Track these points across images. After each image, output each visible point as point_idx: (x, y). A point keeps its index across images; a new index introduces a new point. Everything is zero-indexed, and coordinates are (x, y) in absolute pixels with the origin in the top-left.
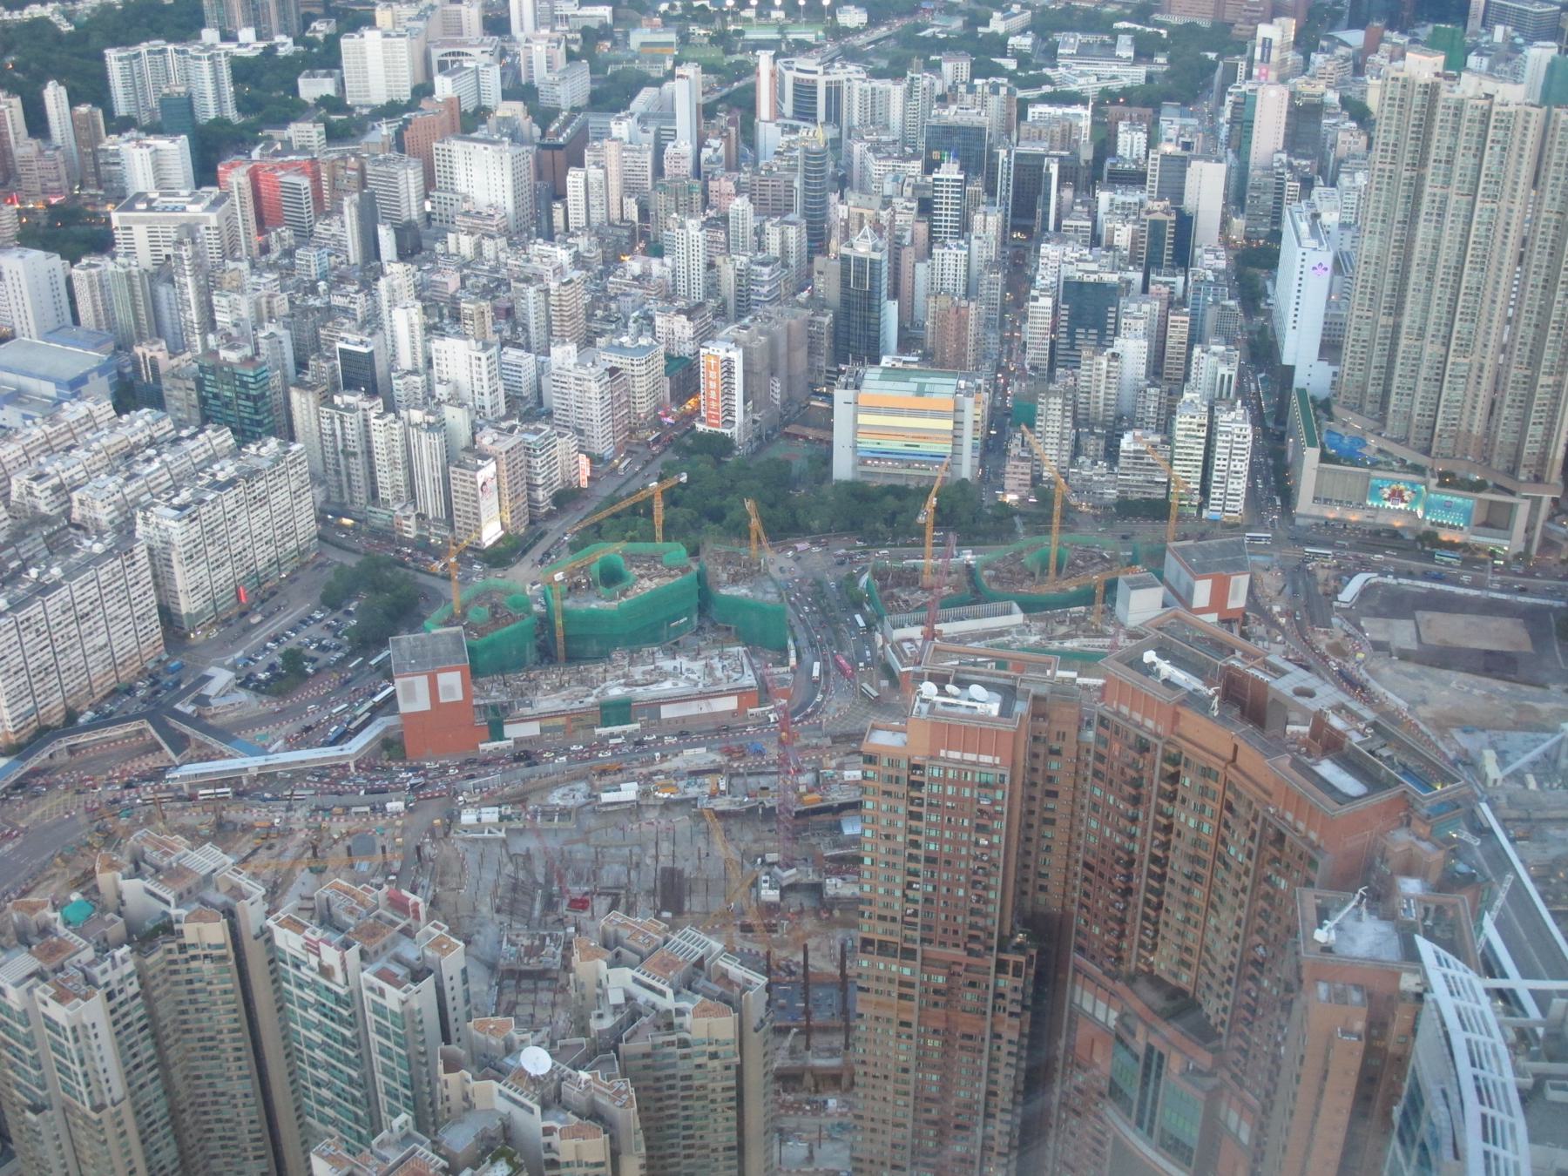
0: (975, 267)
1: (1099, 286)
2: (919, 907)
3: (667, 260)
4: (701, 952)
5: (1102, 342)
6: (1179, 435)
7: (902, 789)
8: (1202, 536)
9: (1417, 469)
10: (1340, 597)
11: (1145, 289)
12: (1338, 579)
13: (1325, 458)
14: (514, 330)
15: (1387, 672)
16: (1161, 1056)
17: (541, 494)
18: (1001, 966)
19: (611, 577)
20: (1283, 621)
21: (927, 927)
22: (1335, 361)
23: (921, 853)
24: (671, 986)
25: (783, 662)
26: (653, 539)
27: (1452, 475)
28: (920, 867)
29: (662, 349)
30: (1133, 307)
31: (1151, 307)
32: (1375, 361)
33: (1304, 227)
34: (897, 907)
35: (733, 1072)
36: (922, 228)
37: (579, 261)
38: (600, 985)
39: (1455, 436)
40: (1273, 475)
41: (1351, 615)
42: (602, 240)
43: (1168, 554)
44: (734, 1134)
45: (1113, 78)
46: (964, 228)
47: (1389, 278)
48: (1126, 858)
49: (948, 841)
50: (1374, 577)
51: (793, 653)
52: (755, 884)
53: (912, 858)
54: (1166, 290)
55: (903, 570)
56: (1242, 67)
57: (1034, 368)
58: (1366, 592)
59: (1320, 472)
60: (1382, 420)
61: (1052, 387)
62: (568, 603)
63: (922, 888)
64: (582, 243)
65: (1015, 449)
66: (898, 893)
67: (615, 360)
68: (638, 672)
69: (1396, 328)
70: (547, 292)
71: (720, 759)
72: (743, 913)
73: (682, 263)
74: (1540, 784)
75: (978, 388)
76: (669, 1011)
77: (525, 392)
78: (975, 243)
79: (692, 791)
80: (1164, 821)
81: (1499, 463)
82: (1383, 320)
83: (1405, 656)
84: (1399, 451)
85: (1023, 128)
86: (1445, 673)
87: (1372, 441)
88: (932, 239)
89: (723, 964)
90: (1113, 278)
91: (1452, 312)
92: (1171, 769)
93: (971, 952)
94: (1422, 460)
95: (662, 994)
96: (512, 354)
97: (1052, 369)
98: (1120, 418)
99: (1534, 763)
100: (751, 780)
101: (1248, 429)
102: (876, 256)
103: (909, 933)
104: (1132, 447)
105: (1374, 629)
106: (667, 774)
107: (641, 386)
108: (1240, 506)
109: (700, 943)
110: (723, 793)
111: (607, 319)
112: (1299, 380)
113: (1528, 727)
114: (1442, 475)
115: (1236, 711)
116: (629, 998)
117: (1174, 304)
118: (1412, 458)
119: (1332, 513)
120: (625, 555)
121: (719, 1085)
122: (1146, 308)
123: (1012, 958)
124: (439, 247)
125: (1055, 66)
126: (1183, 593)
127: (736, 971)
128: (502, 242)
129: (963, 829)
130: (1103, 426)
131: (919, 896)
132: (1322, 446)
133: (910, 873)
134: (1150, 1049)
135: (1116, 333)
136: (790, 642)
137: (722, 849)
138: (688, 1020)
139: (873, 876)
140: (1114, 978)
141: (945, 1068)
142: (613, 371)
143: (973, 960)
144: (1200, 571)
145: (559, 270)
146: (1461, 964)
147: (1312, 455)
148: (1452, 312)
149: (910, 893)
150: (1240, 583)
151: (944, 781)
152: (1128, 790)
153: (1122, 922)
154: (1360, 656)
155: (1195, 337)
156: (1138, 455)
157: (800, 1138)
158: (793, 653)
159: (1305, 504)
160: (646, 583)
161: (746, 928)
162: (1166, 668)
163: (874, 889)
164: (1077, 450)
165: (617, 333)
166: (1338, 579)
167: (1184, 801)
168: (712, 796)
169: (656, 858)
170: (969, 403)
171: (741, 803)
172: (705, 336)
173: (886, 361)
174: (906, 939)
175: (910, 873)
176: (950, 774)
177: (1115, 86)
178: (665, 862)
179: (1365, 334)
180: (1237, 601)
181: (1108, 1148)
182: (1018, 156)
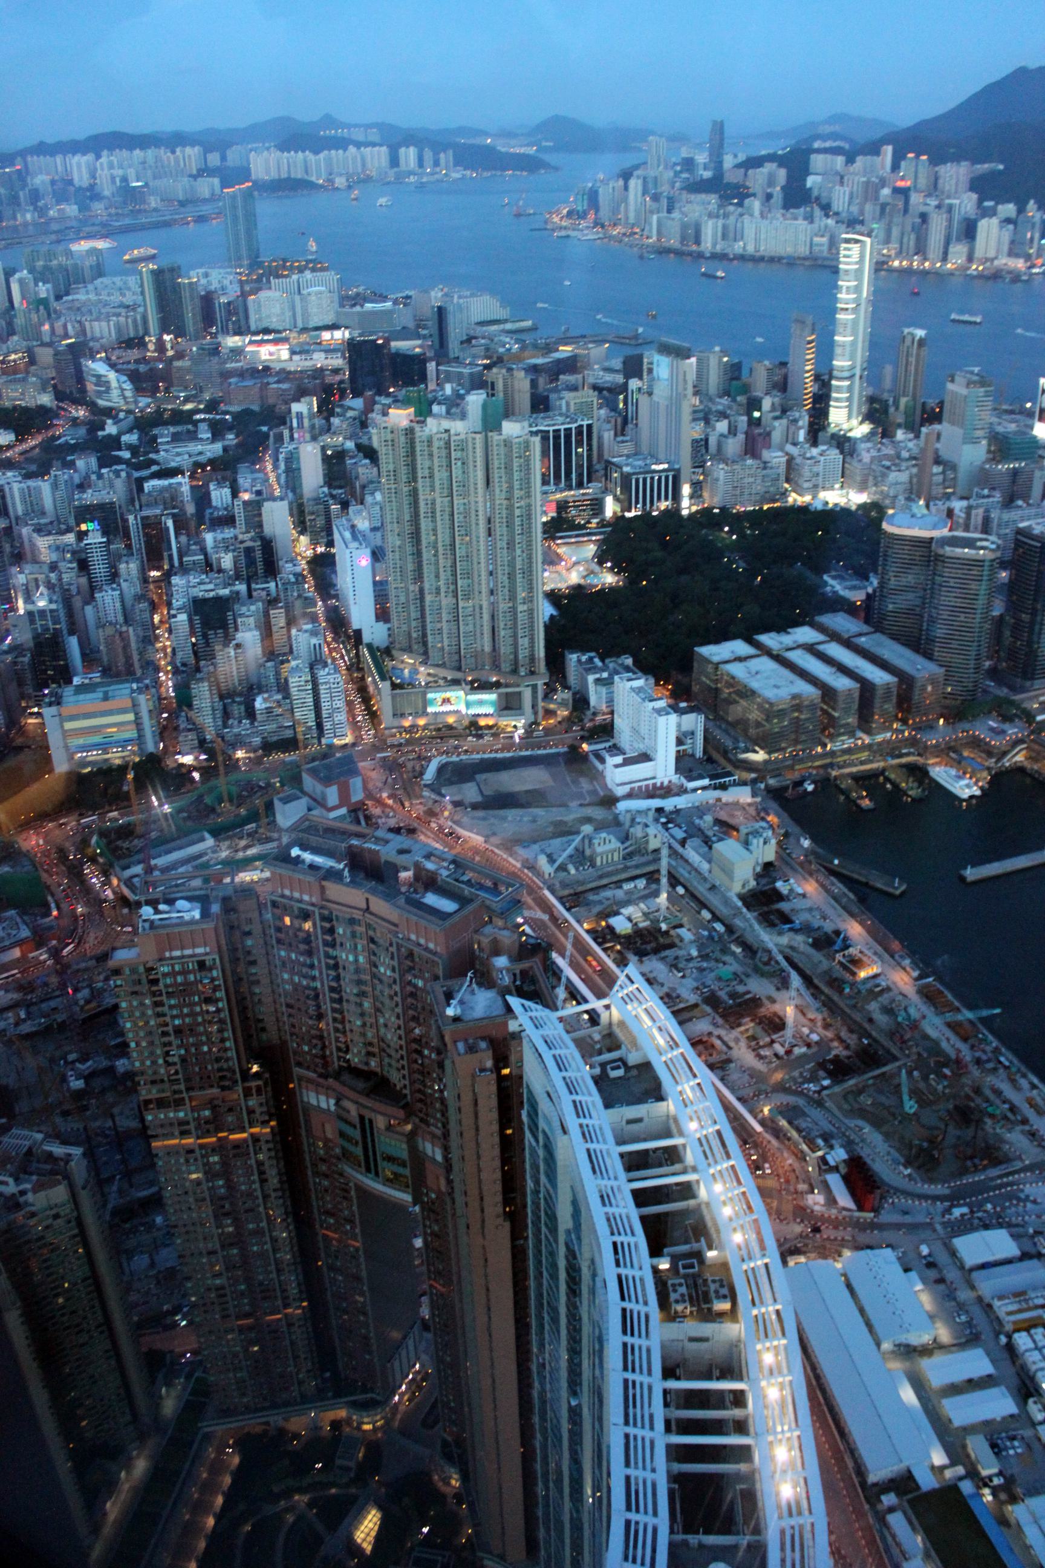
1: (218, 599)
2: (178, 1067)
4: (27, 1143)
5: (227, 639)
6: (294, 691)
7: (145, 988)
10: (425, 777)
11: (250, 596)
15: (465, 820)
16: (371, 1121)
18: (247, 1093)
20: (390, 802)
21: (187, 1080)
23: (170, 1029)
24: (11, 1175)
25: (48, 913)
28: (172, 1038)
30: (244, 609)
32: (413, 615)
33: (347, 535)
34: (162, 1071)
35: (73, 1223)
36: (83, 580)
43: (305, 776)
44: (86, 1268)
45: (200, 453)
46: (114, 576)
47: (410, 559)
48: (312, 993)
49: (187, 1015)
50: (444, 759)
51: (53, 905)
52: (64, 1079)
53: (165, 1034)
54: (264, 593)
56: (286, 433)
57: (184, 665)
58: (441, 769)
59: (394, 697)
61: (198, 676)
63: (176, 1053)
66: (161, 1061)
69: (422, 591)
71: (16, 996)
72: (61, 1103)
74: (577, 869)
75: (147, 687)
76: (13, 1195)
78: (124, 585)
80: (332, 962)
81: (506, 667)
82: (411, 588)
83: (475, 807)
85: (144, 499)
86: (502, 812)
88: (92, 588)
89: (47, 1148)
90: (225, 592)
92: (327, 925)
93: (223, 1088)
94: (458, 675)
95: (6, 1183)
98: (251, 688)
99: (571, 856)
100: (43, 1005)
102: (53, 606)
103: (176, 1087)
104: (264, 706)
109: (25, 1138)
110: (24, 1020)
112: (366, 638)
114: (472, 682)
115: (362, 875)
117: (272, 602)
122: (253, 608)
123: (253, 1084)
125: (157, 452)
126: (319, 799)
127: (58, 1150)
129: (196, 1004)
130: (240, 695)
131: (176, 1059)
133: (165, 1045)
134: (362, 1118)
135: (236, 629)
136: (49, 898)
137: (31, 1062)
138: (30, 1197)
139: (141, 1053)
144: (327, 781)
146: (539, 1007)
148: (454, 574)
149: (170, 1059)
151: (173, 974)
152: (303, 947)
154: (446, 813)
156: (269, 710)
157: (142, 1252)
158: (53, 905)
161: (65, 1114)
162: (308, 857)
163: (143, 1063)
164: (226, 715)
167: (342, 944)
168: (17, 1024)
170: (142, 699)
171: (40, 1024)
173: (76, 681)
174: (175, 1092)
176: (177, 968)
177: (202, 459)
181: (353, 1193)
182: (143, 518)
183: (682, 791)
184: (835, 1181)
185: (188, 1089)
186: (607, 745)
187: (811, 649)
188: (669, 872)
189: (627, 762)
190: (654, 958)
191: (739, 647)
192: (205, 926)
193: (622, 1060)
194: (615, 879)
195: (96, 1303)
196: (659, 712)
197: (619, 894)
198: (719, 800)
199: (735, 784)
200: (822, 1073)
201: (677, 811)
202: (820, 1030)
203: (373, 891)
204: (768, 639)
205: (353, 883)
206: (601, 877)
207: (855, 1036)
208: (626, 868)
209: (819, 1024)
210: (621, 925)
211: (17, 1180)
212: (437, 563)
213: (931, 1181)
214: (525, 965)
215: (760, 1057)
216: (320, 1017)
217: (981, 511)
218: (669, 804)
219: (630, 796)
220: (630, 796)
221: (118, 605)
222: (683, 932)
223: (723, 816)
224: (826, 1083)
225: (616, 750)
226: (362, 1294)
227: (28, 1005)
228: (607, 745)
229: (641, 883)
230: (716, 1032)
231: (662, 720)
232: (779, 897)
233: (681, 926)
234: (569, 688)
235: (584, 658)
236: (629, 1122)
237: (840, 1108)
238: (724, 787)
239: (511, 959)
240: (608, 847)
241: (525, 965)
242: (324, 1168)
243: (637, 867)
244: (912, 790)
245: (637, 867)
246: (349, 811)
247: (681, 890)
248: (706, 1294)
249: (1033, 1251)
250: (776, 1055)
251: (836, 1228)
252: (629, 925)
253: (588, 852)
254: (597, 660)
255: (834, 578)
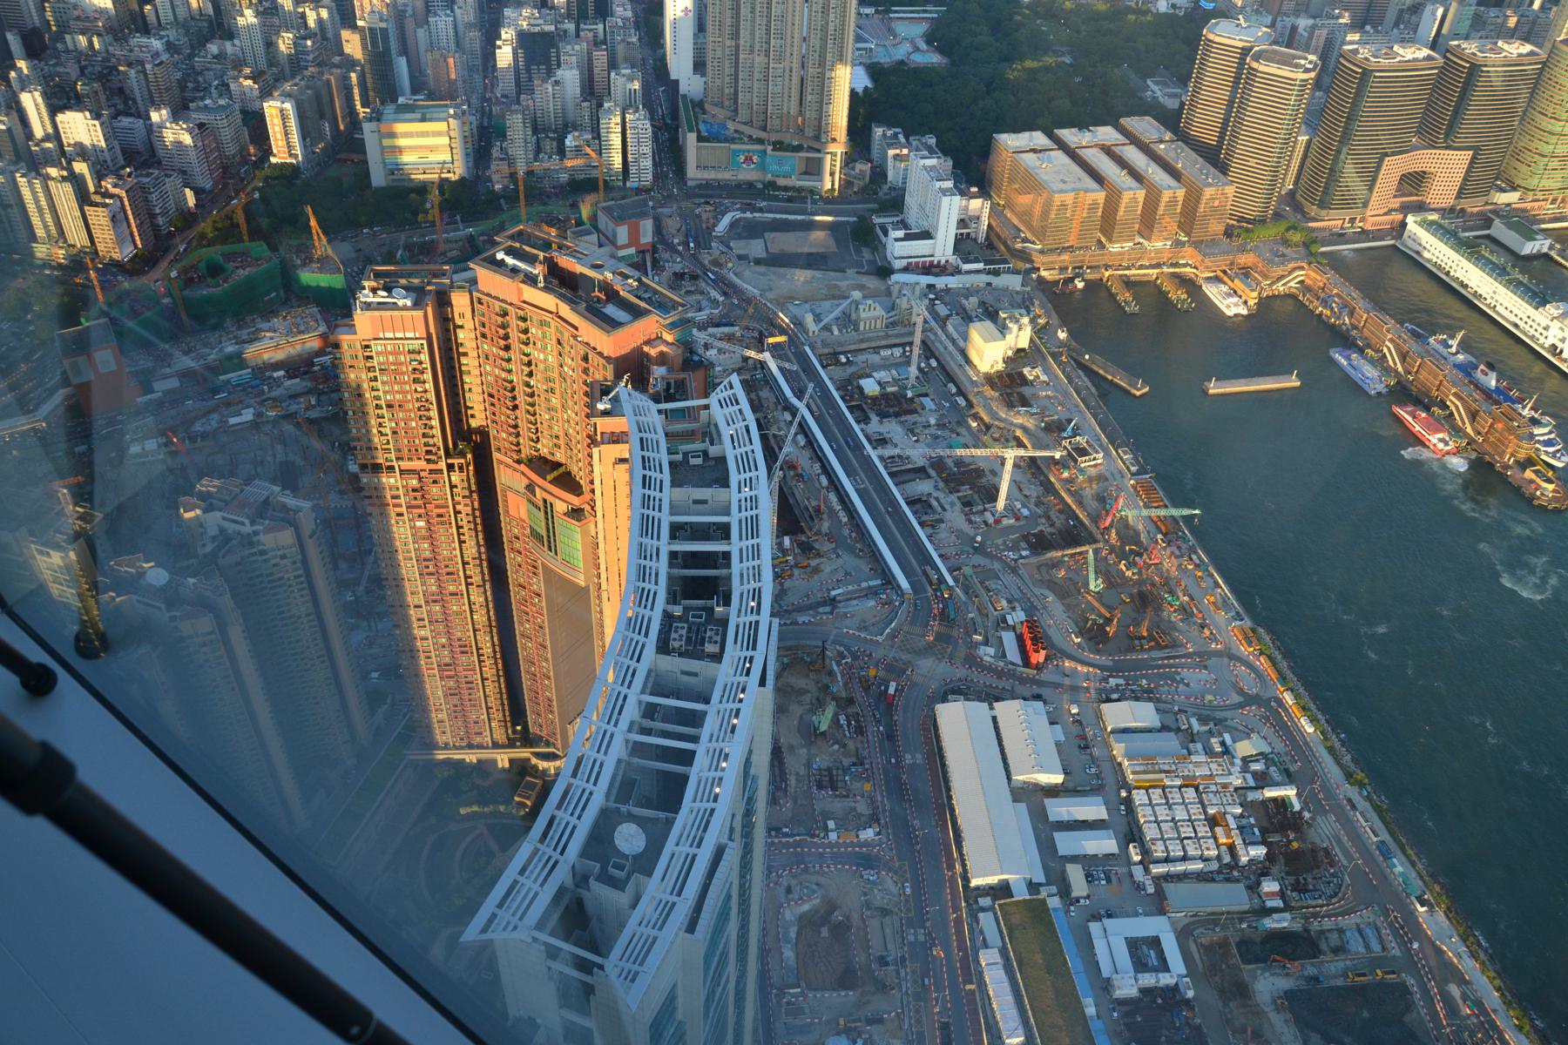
0: (461, 28)
1: (544, 35)
3: (236, 42)
5: (550, 73)
8: (624, 198)
9: (760, 141)
11: (578, 36)
12: (715, 217)
13: (700, 139)
14: (125, 102)
15: (747, 273)
17: (160, 220)
18: (450, 467)
19: (215, 270)
22: (703, 75)
23: (383, 403)
26: (241, 240)
27: (781, 143)
28: (384, 411)
29: (237, 107)
31: (581, 47)
32: (727, 71)
37: (170, 47)
38: (201, 525)
39: (780, 117)
40: (669, 152)
41: (724, 241)
42: (187, 32)
47: (729, 14)
50: (738, 215)
55: (425, 243)
58: (733, 225)
59: (698, 148)
60: (736, 111)
62: (187, 292)
63: (389, 426)
64: (172, 34)
65: (496, 152)
67: (202, 117)
68: (244, 334)
69: (737, 46)
70: (144, 72)
73: (247, 43)
75: (464, 112)
77: (140, 148)
78: (458, 11)
79: (294, 408)
80: (526, 359)
81: (809, 132)
82: (728, 43)
83: (758, 262)
84: (747, 130)
87: (731, 126)
90: (552, 28)
91: (768, 33)
93: (428, 461)
95: (243, 524)
96: (126, 121)
97: (519, 93)
98: (566, 126)
101: (648, 125)
102: (383, 25)
105: (739, 247)
106: (274, 400)
107: (226, 135)
108: (650, 177)
111: (196, 89)
112: (683, 89)
113: (834, 297)
114: (774, 144)
115: (556, 282)
116: (222, 530)
117: (596, 43)
118: (757, 134)
119: (711, 175)
120: (223, 255)
121: (291, 575)
122: (577, 47)
123: (455, 462)
124: (60, 46)
126: (610, 235)
127: (290, 501)
128: (109, 38)
132: (699, 132)
133: (379, 417)
134: (545, 501)
135: (559, 66)
138: (262, 537)
140: (519, 462)
141: (431, 537)
142: (201, 126)
143: (433, 467)
144: (619, 220)
145: (156, 54)
147: (692, 138)
148: (768, 33)
150: (647, 226)
151: (387, 353)
152: (502, 343)
153: (516, 427)
155: (613, 65)
159: (692, 172)
160: (241, 272)
162: (510, 261)
163: (359, 430)
165: (202, 99)
166: (715, 217)
168: (307, 409)
169: (274, 456)
172: (266, 93)
173: (401, 100)
175: (379, 417)
178: (280, 457)
179: (719, 53)
180: (647, 237)
183: (957, 271)
184: (1009, 639)
185: (398, 459)
186: (895, 219)
187: (1108, 151)
188: (923, 342)
189: (908, 237)
190: (893, 420)
191: (1039, 139)
192: (414, 313)
193: (705, 453)
194: (874, 344)
195: (318, 636)
196: (944, 192)
197: (875, 359)
198: (989, 284)
199: (1009, 271)
200: (1023, 545)
201: (947, 290)
202: (1032, 506)
203: (562, 297)
204: (1069, 135)
205: (546, 289)
206: (862, 341)
207: (1062, 517)
208: (887, 336)
209: (1033, 500)
210: (870, 386)
211: (253, 523)
212: (753, 21)
213: (1098, 652)
214: (682, 375)
215: (970, 521)
216: (515, 407)
217: (1324, 32)
218: (941, 282)
219: (906, 270)
220: (906, 270)
221: (451, 31)
222: (927, 401)
223: (989, 299)
224: (1024, 553)
225: (904, 225)
226: (546, 660)
227: (320, 394)
228: (895, 219)
229: (898, 352)
230: (935, 495)
231: (946, 200)
232: (1024, 381)
233: (926, 395)
234: (870, 161)
235: (889, 133)
236: (696, 502)
237: (1031, 577)
238: (996, 273)
239: (670, 370)
240: (872, 314)
241: (682, 375)
242: (517, 545)
243: (896, 336)
244: (1178, 295)
245: (896, 336)
246: (638, 252)
247: (934, 363)
248: (703, 639)
249: (1174, 726)
250: (985, 523)
251: (999, 677)
252: (878, 388)
253: (854, 316)
254: (901, 136)
255: (1156, 83)
